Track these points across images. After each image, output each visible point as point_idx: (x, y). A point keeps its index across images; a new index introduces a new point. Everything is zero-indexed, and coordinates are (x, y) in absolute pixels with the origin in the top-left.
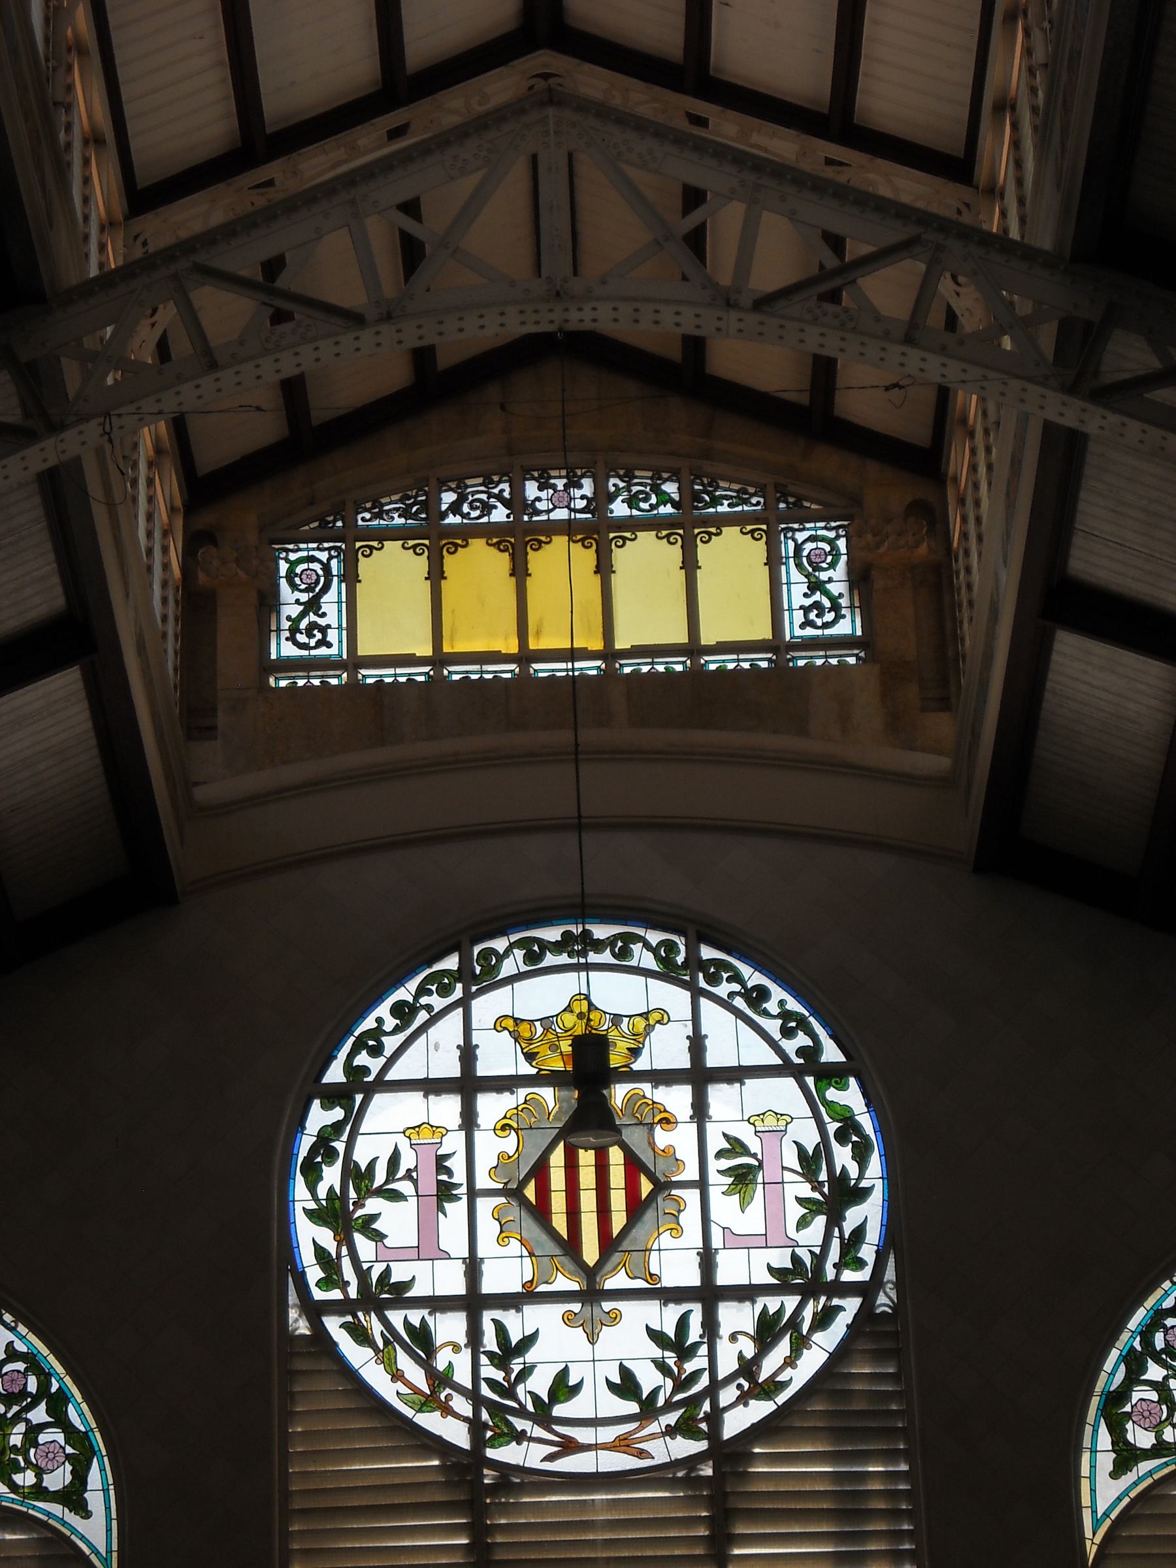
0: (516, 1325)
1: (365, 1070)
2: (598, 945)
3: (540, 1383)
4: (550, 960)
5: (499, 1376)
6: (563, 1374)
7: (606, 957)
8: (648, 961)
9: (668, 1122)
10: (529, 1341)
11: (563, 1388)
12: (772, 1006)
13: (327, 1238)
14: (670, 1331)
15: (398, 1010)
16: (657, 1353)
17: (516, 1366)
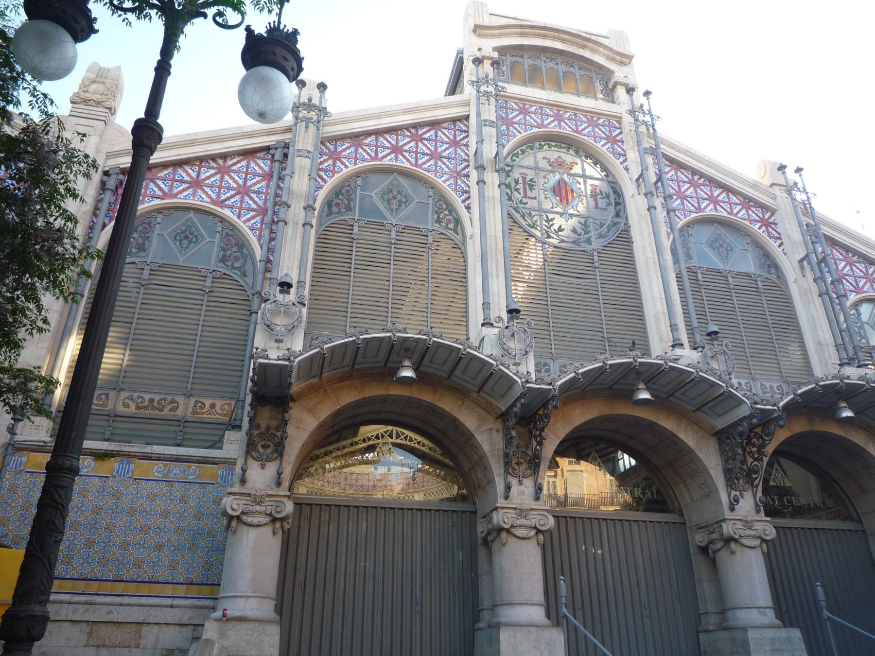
0: (550, 216)
1: (515, 160)
2: (563, 148)
3: (556, 227)
4: (553, 148)
5: (547, 224)
6: (560, 227)
7: (564, 150)
8: (573, 153)
9: (579, 183)
10: (553, 219)
11: (560, 229)
13: (508, 191)
14: (583, 222)
15: (521, 150)
16: (580, 226)
17: (551, 223)
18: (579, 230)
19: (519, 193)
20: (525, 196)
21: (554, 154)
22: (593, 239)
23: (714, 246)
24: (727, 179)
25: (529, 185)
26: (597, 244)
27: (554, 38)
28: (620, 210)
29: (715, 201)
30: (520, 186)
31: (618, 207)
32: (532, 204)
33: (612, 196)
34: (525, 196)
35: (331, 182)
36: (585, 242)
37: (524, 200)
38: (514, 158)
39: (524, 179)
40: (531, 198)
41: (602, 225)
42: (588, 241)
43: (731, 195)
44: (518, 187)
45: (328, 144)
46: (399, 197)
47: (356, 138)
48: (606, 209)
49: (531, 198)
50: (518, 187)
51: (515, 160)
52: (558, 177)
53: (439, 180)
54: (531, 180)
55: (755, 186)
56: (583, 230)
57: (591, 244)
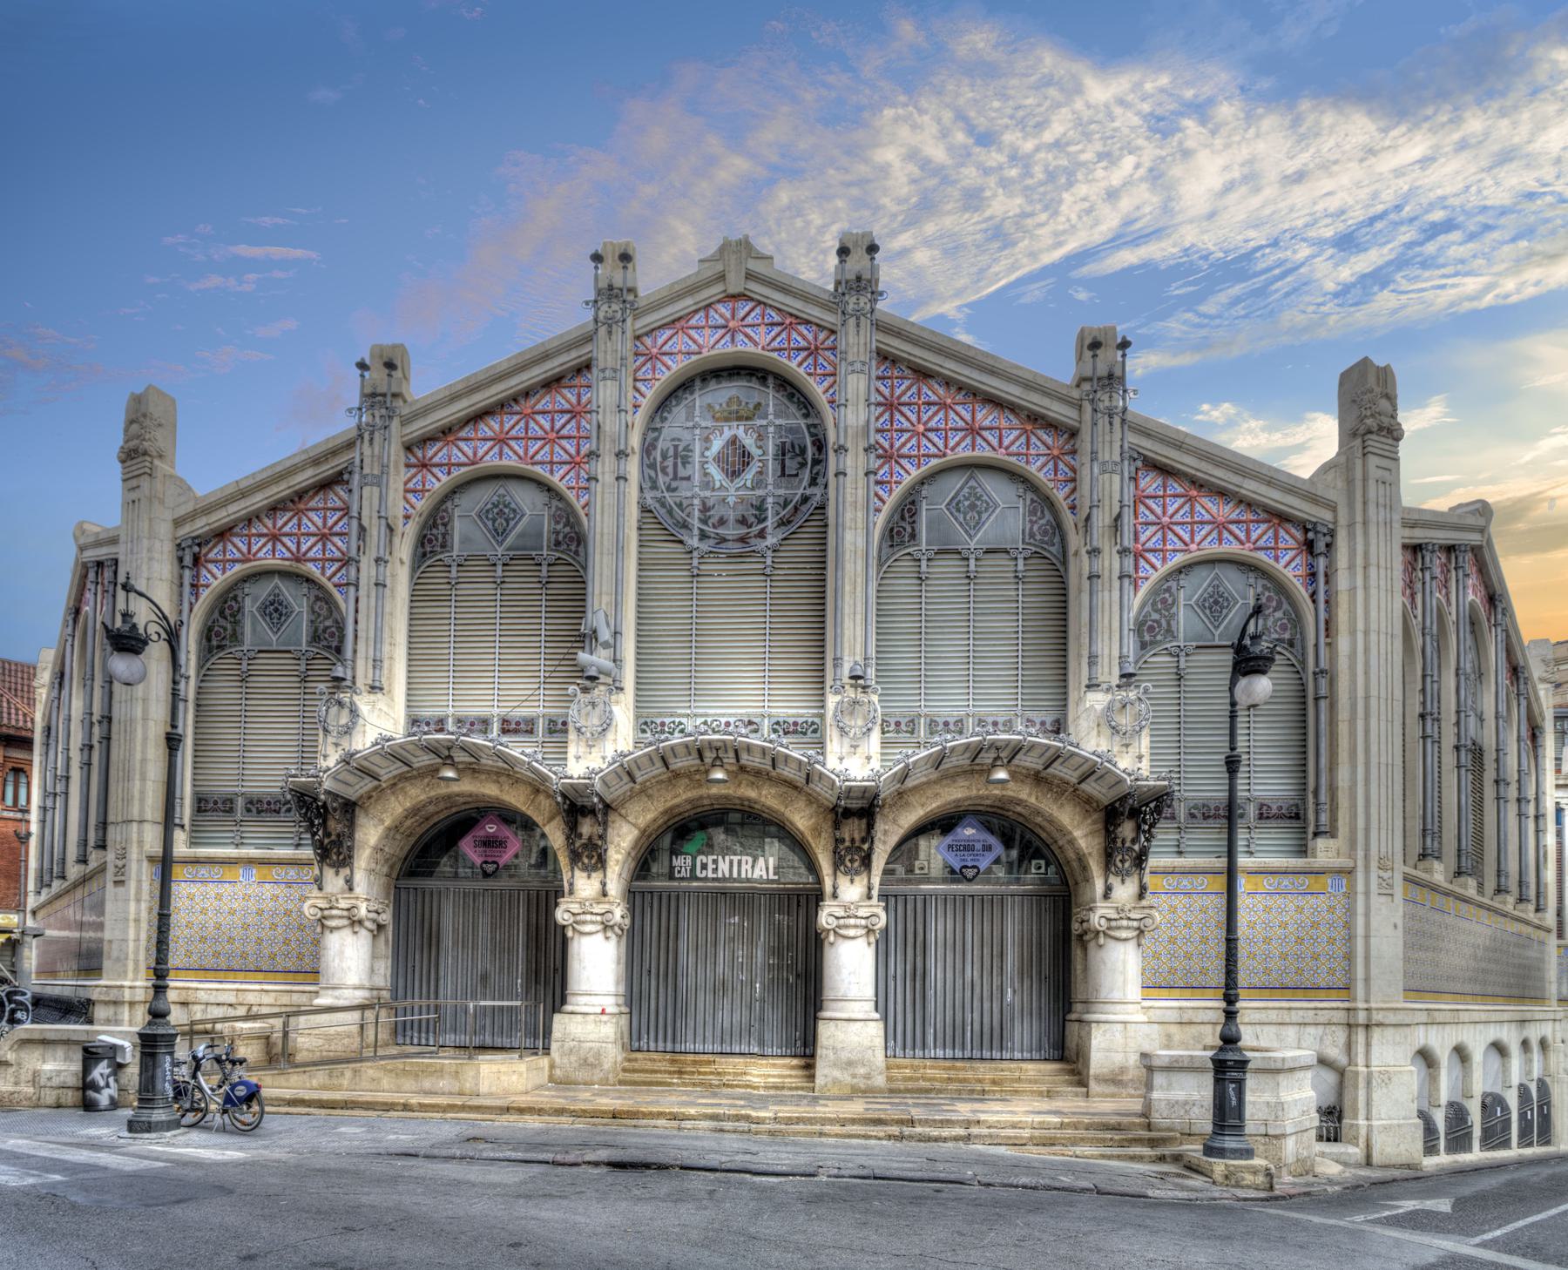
12: (795, 400)
18: (752, 519)
20: (675, 478)
21: (723, 394)
22: (769, 530)
25: (682, 457)
26: (771, 540)
28: (817, 474)
29: (973, 431)
30: (670, 463)
31: (818, 467)
34: (675, 478)
35: (422, 505)
36: (755, 536)
37: (674, 484)
38: (665, 414)
39: (676, 447)
40: (683, 479)
41: (786, 504)
42: (762, 535)
44: (666, 464)
45: (416, 450)
48: (797, 475)
49: (683, 479)
50: (666, 464)
51: (666, 418)
52: (728, 434)
54: (686, 449)
56: (756, 516)
57: (764, 538)
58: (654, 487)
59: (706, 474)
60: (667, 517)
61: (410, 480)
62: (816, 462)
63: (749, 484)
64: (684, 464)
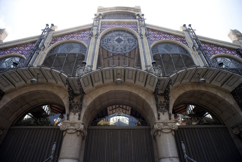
11: (117, 49)
13: (103, 42)
18: (123, 48)
19: (106, 42)
23: (166, 48)
24: (169, 31)
27: (119, 9)
28: (136, 43)
29: (166, 37)
31: (135, 42)
32: (109, 44)
33: (134, 40)
37: (107, 43)
39: (108, 39)
40: (109, 43)
43: (171, 35)
46: (71, 47)
47: (62, 36)
48: (132, 43)
49: (109, 43)
52: (118, 37)
53: (83, 42)
55: (177, 32)
58: (103, 43)
59: (114, 42)
60: (106, 48)
61: (52, 42)
62: (135, 41)
63: (122, 44)
64: (110, 41)
